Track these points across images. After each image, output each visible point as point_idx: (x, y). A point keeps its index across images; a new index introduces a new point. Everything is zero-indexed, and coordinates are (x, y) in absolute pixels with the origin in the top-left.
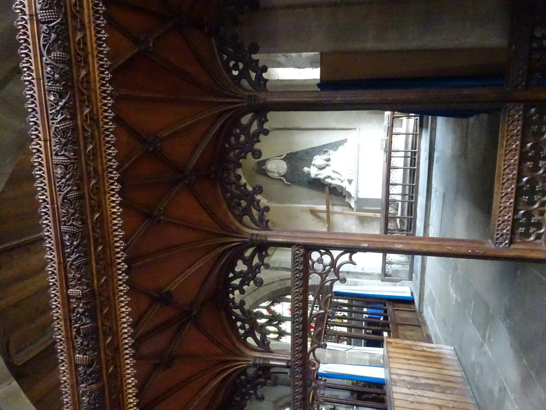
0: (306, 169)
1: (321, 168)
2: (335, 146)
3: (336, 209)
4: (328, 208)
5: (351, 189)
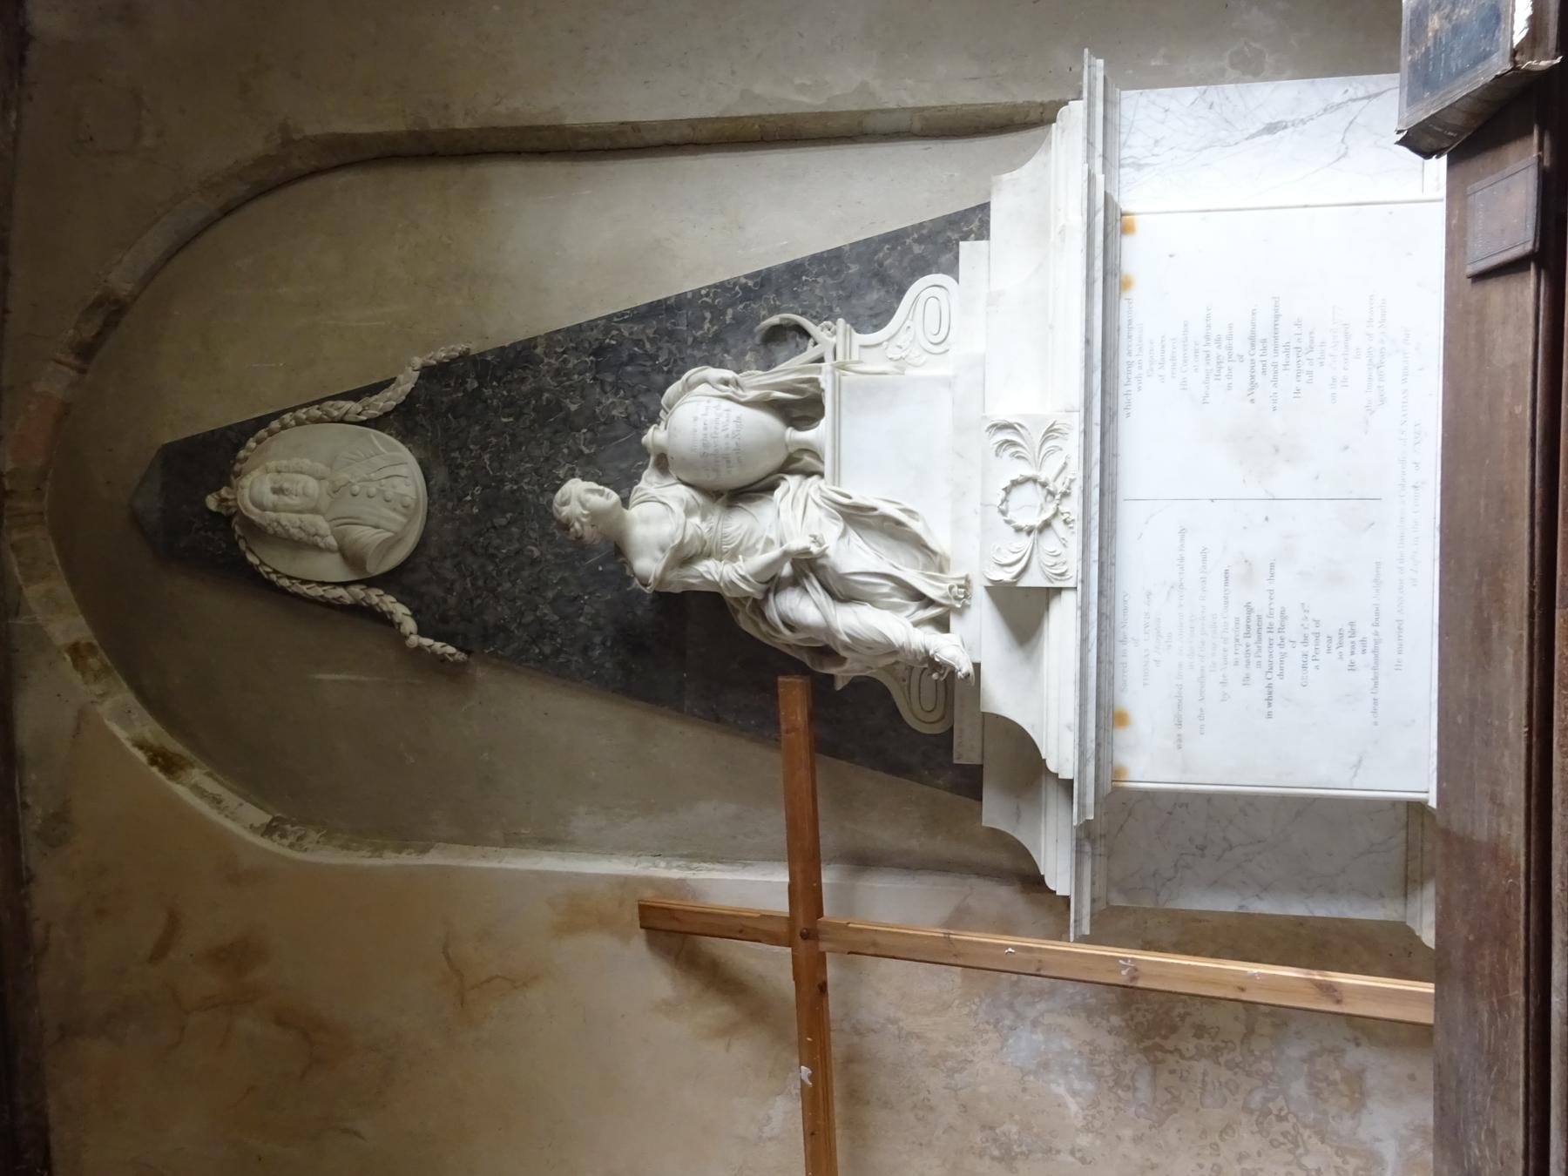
0: (580, 497)
2: (872, 278)
3: (890, 903)
4: (806, 892)
5: (1039, 697)
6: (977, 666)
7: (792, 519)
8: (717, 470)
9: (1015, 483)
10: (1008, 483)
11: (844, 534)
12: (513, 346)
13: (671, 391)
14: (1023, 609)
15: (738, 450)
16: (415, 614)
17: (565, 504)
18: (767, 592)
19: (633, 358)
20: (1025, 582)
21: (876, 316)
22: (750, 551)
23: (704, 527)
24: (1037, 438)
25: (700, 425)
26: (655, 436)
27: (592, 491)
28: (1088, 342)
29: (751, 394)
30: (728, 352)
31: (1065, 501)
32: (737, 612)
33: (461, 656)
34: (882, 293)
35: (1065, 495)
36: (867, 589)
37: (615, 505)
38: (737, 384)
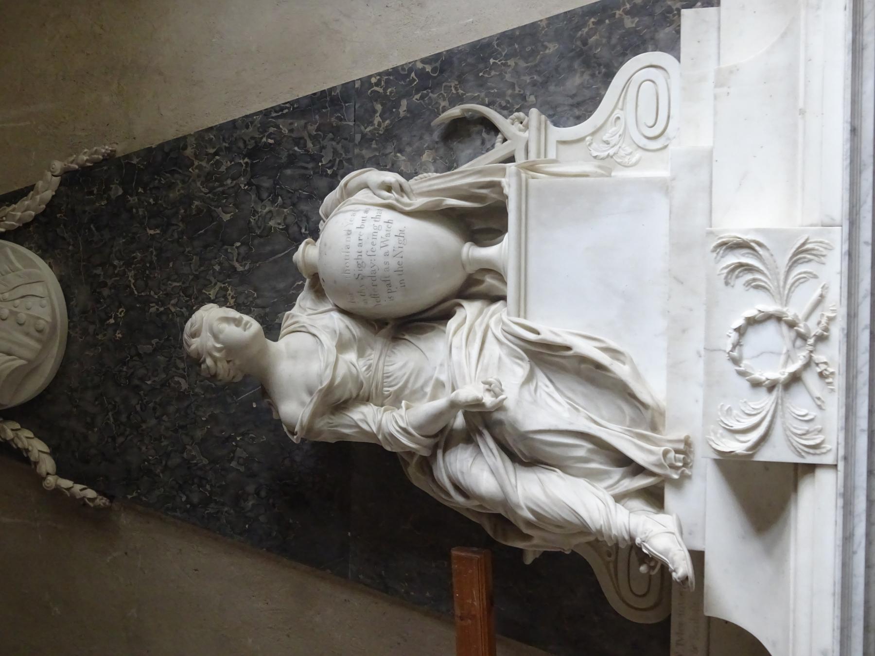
0: (216, 326)
1: (403, 318)
6: (698, 558)
7: (467, 361)
8: (375, 296)
9: (752, 322)
10: (739, 322)
11: (530, 378)
12: (161, 146)
13: (329, 198)
14: (764, 492)
15: (400, 271)
16: (54, 452)
17: (194, 335)
18: (436, 447)
19: (292, 160)
20: (766, 455)
21: (578, 105)
22: (417, 395)
23: (361, 365)
24: (783, 262)
25: (354, 240)
26: (307, 252)
27: (227, 320)
28: (854, 131)
29: (418, 202)
30: (401, 151)
31: (821, 347)
32: (407, 464)
33: (102, 501)
34: (586, 77)
35: (821, 339)
36: (557, 451)
37: (255, 337)
38: (402, 190)
